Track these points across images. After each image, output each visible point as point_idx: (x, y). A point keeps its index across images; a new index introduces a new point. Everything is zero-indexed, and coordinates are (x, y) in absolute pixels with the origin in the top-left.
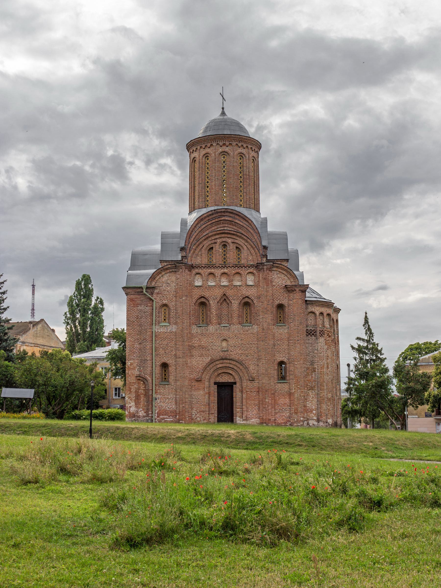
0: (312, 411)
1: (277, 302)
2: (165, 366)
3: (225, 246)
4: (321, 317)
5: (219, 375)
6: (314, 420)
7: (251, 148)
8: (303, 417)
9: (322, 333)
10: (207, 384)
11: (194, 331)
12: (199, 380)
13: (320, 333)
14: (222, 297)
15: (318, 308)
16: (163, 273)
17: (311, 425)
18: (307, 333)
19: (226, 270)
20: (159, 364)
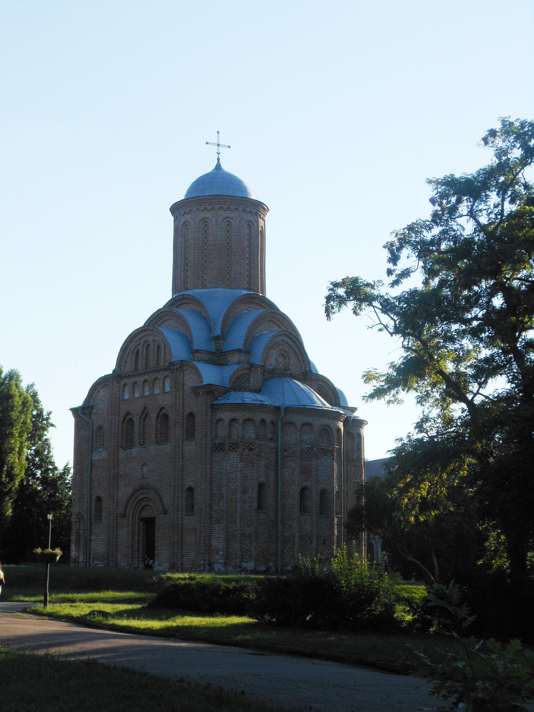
0: (218, 552)
1: (188, 411)
2: (99, 499)
3: (148, 345)
4: (236, 425)
5: (143, 508)
6: (221, 563)
7: (221, 207)
8: (204, 560)
9: (234, 447)
10: (131, 520)
11: (121, 456)
12: (124, 516)
13: (231, 446)
14: (143, 411)
15: (227, 414)
16: (99, 388)
17: (216, 570)
18: (215, 447)
19: (146, 377)
20: (94, 498)
